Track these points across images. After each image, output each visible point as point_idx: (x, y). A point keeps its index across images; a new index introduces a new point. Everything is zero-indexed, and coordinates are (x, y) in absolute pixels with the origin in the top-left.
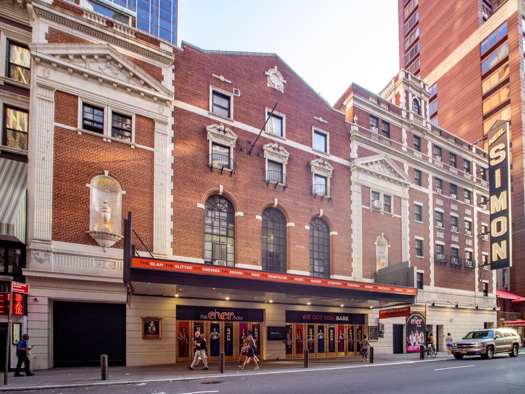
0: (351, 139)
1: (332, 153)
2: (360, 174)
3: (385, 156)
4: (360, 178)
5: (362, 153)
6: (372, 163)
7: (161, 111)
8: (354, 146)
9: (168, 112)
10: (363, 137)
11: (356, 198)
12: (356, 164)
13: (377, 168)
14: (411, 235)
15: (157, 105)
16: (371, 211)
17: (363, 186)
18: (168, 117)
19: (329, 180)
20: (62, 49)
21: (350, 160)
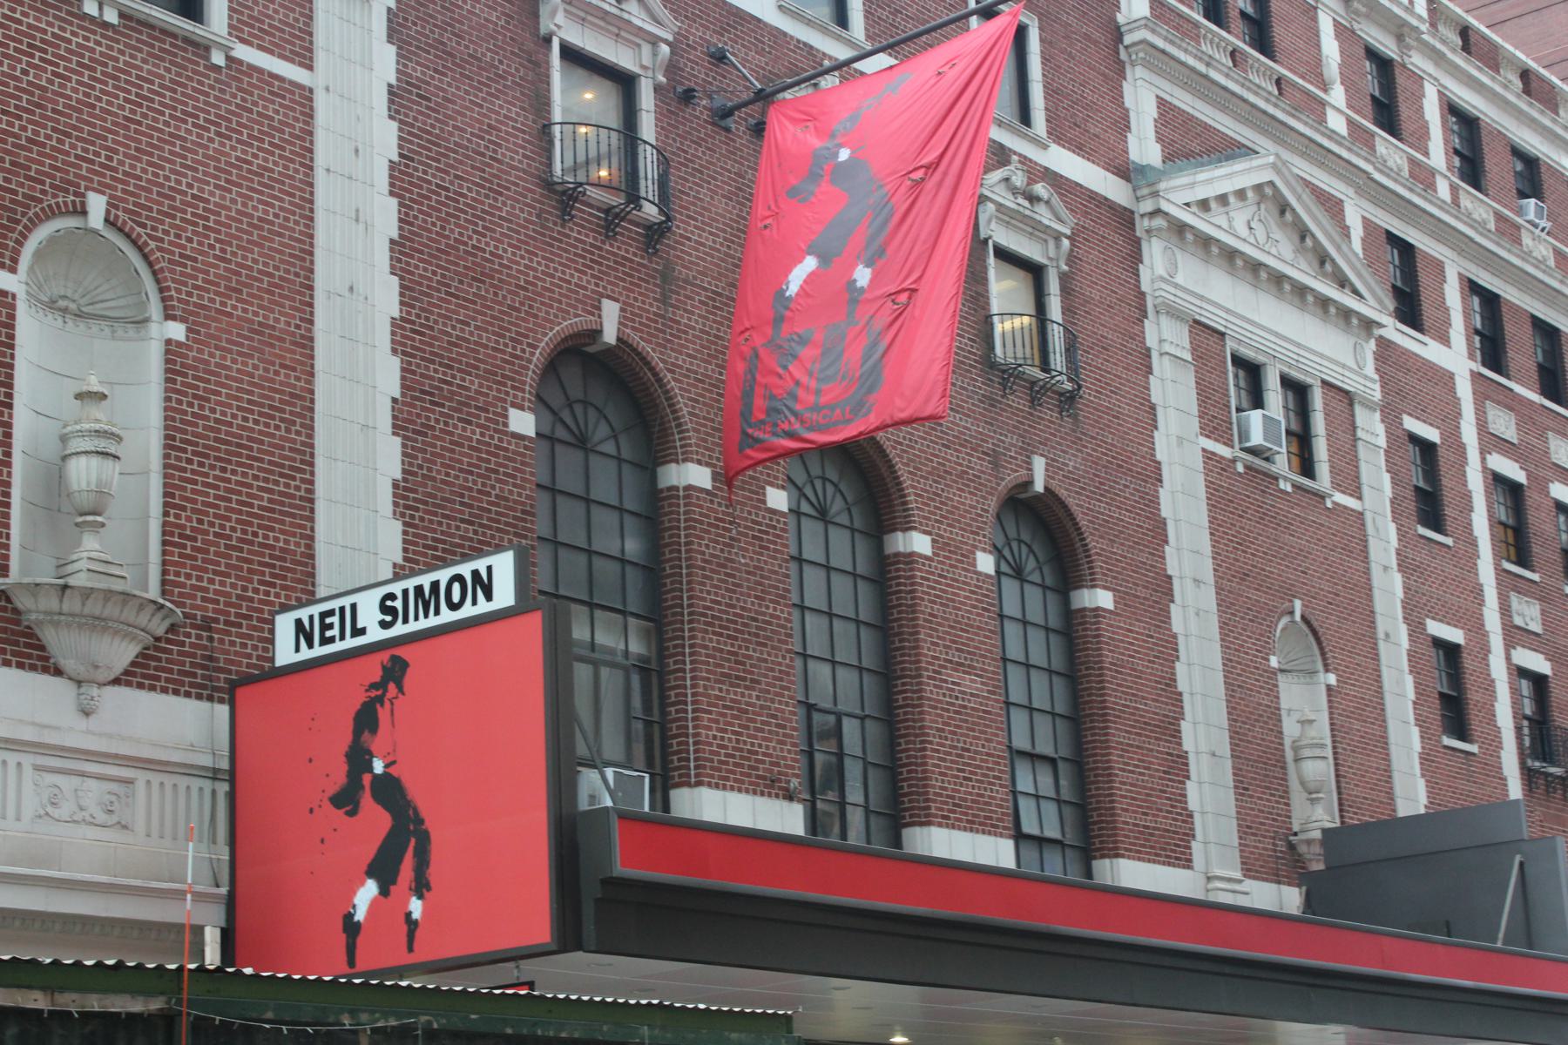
0: (1123, 55)
1: (1059, 133)
2: (1180, 256)
3: (1274, 166)
4: (1179, 279)
5: (1188, 143)
6: (1223, 199)
8: (1142, 97)
10: (1182, 56)
11: (1173, 391)
12: (1165, 206)
13: (1238, 227)
14: (1414, 614)
16: (1240, 468)
17: (1200, 328)
19: (1053, 286)
21: (1124, 170)
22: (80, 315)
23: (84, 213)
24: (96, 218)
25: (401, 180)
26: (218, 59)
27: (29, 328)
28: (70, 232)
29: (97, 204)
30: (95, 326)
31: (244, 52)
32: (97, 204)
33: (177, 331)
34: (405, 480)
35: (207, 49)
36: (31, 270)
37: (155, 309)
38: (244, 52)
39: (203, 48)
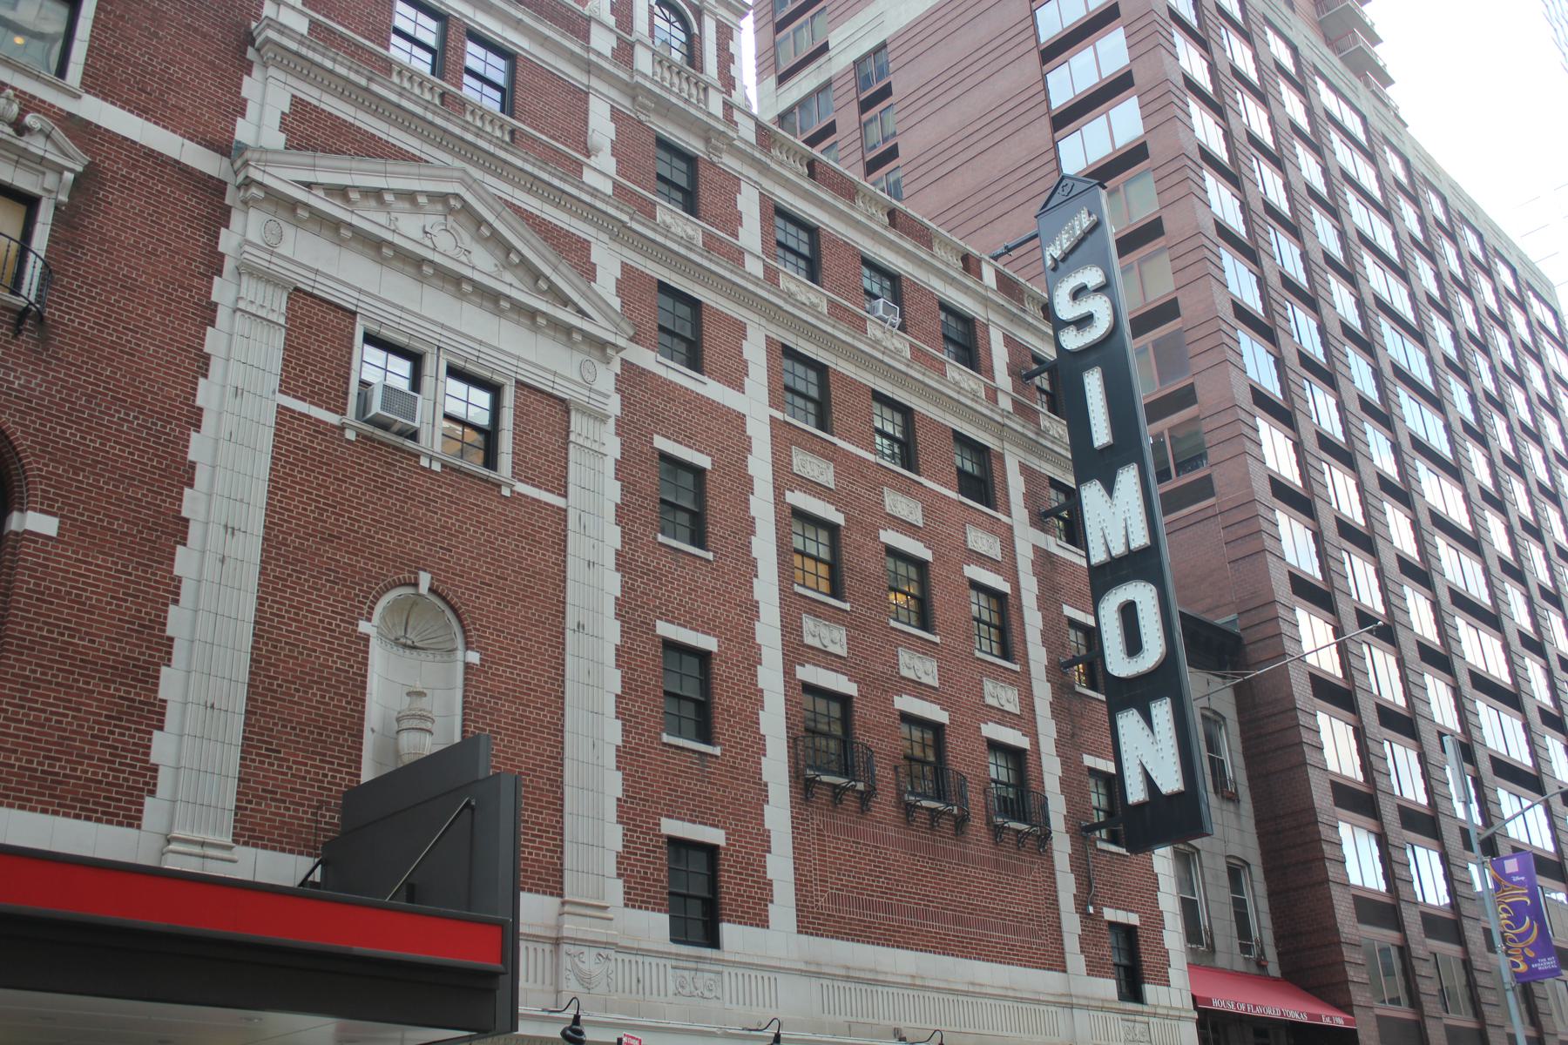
7: (589, 378)
9: (606, 378)
15: (578, 357)
18: (607, 396)
20: (333, 171)
22: (414, 648)
23: (416, 585)
24: (424, 587)
25: (623, 563)
26: (506, 492)
27: (378, 656)
28: (407, 597)
29: (425, 579)
30: (423, 654)
31: (522, 488)
32: (425, 579)
33: (474, 657)
35: (499, 486)
36: (383, 618)
37: (460, 642)
38: (522, 488)
39: (498, 485)
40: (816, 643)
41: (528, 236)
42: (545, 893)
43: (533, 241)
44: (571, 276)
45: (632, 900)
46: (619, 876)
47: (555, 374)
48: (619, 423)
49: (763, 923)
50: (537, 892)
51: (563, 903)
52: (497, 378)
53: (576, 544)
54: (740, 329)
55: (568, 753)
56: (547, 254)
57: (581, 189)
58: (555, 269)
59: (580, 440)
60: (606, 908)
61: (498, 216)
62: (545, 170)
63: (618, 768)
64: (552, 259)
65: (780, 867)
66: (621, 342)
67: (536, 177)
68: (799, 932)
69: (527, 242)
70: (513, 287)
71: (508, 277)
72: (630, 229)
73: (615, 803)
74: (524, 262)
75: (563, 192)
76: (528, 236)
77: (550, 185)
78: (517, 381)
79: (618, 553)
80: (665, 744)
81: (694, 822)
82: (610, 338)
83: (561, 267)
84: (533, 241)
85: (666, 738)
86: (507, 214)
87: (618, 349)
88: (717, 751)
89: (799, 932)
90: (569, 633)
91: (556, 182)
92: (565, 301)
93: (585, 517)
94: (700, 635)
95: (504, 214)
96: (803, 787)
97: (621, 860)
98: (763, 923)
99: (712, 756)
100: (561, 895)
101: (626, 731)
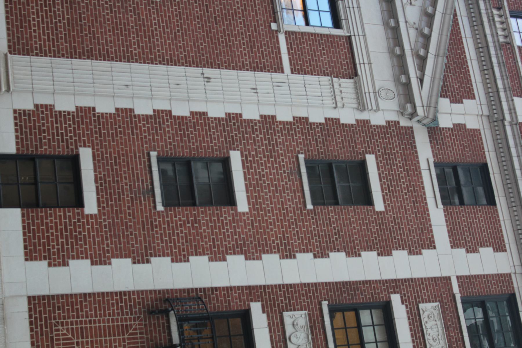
7: (383, 94)
15: (391, 85)
26: (274, 26)
34: (135, 116)
40: (289, 330)
41: (445, 33)
42: (9, 41)
43: (444, 37)
44: (439, 66)
45: (20, 116)
46: (36, 106)
47: (370, 64)
48: (365, 123)
49: (30, 255)
50: (9, 35)
51: (6, 55)
52: (344, 23)
53: (263, 79)
54: (499, 246)
55: (115, 64)
56: (442, 48)
57: (508, 101)
58: (437, 56)
59: (336, 86)
60: (8, 90)
61: (444, 14)
62: (496, 50)
63: (117, 110)
64: (442, 52)
65: (80, 277)
66: (420, 111)
67: (488, 47)
68: (31, 299)
69: (441, 34)
70: (409, 39)
71: (413, 33)
72: (504, 126)
73: (91, 105)
74: (427, 38)
75: (493, 69)
76: (445, 33)
77: (490, 58)
78: (349, 37)
79: (273, 117)
80: (149, 155)
81: (96, 182)
82: (418, 102)
83: (440, 59)
84: (444, 37)
85: (154, 154)
86: (449, 18)
87: (413, 114)
88: (160, 207)
89: (31, 299)
90: (199, 70)
91: (494, 60)
92: (422, 68)
93: (285, 87)
94: (244, 194)
95: (447, 17)
96: (160, 304)
97: (49, 108)
98: (30, 255)
99: (154, 202)
100: (10, 53)
101: (147, 117)
